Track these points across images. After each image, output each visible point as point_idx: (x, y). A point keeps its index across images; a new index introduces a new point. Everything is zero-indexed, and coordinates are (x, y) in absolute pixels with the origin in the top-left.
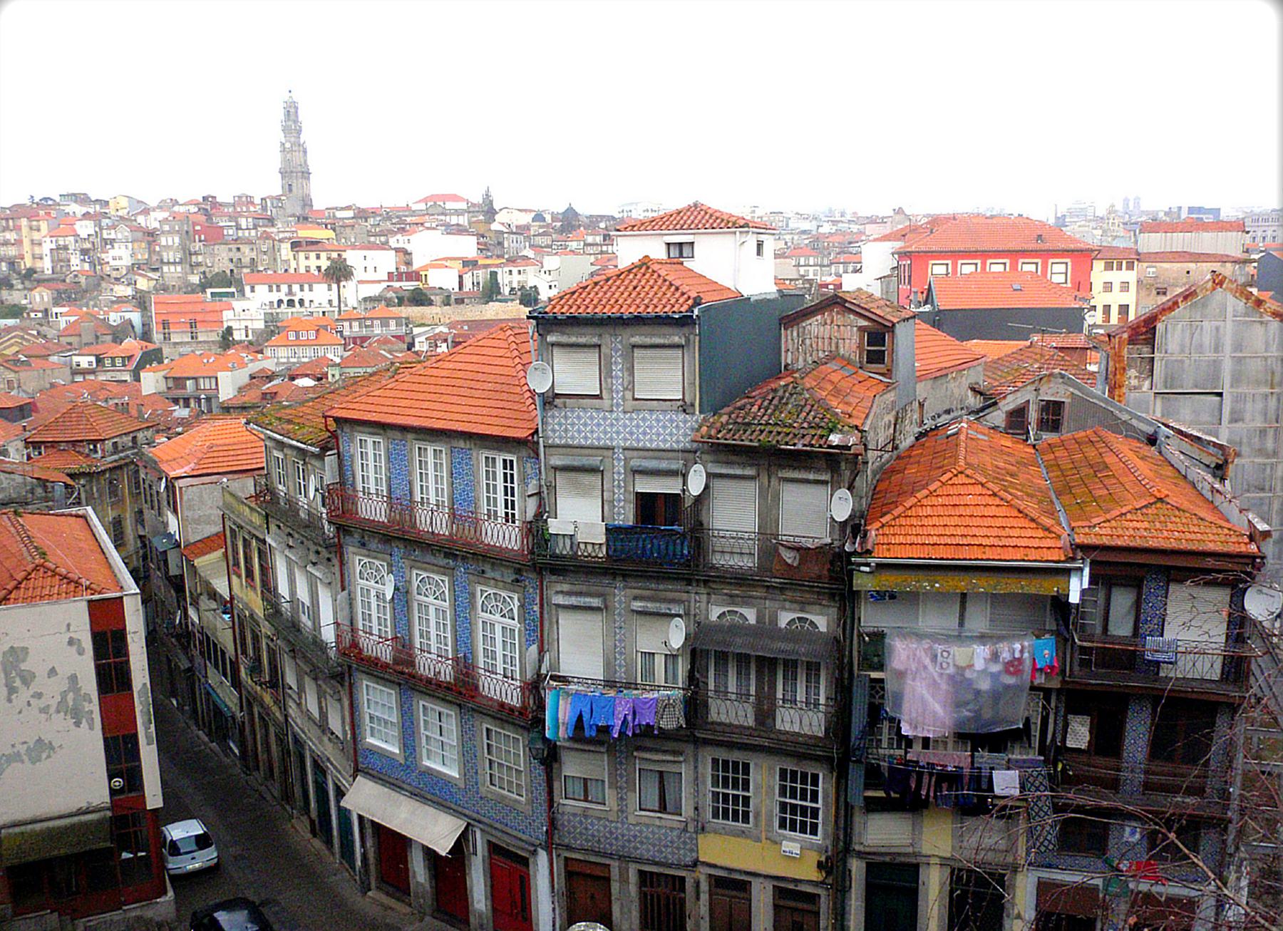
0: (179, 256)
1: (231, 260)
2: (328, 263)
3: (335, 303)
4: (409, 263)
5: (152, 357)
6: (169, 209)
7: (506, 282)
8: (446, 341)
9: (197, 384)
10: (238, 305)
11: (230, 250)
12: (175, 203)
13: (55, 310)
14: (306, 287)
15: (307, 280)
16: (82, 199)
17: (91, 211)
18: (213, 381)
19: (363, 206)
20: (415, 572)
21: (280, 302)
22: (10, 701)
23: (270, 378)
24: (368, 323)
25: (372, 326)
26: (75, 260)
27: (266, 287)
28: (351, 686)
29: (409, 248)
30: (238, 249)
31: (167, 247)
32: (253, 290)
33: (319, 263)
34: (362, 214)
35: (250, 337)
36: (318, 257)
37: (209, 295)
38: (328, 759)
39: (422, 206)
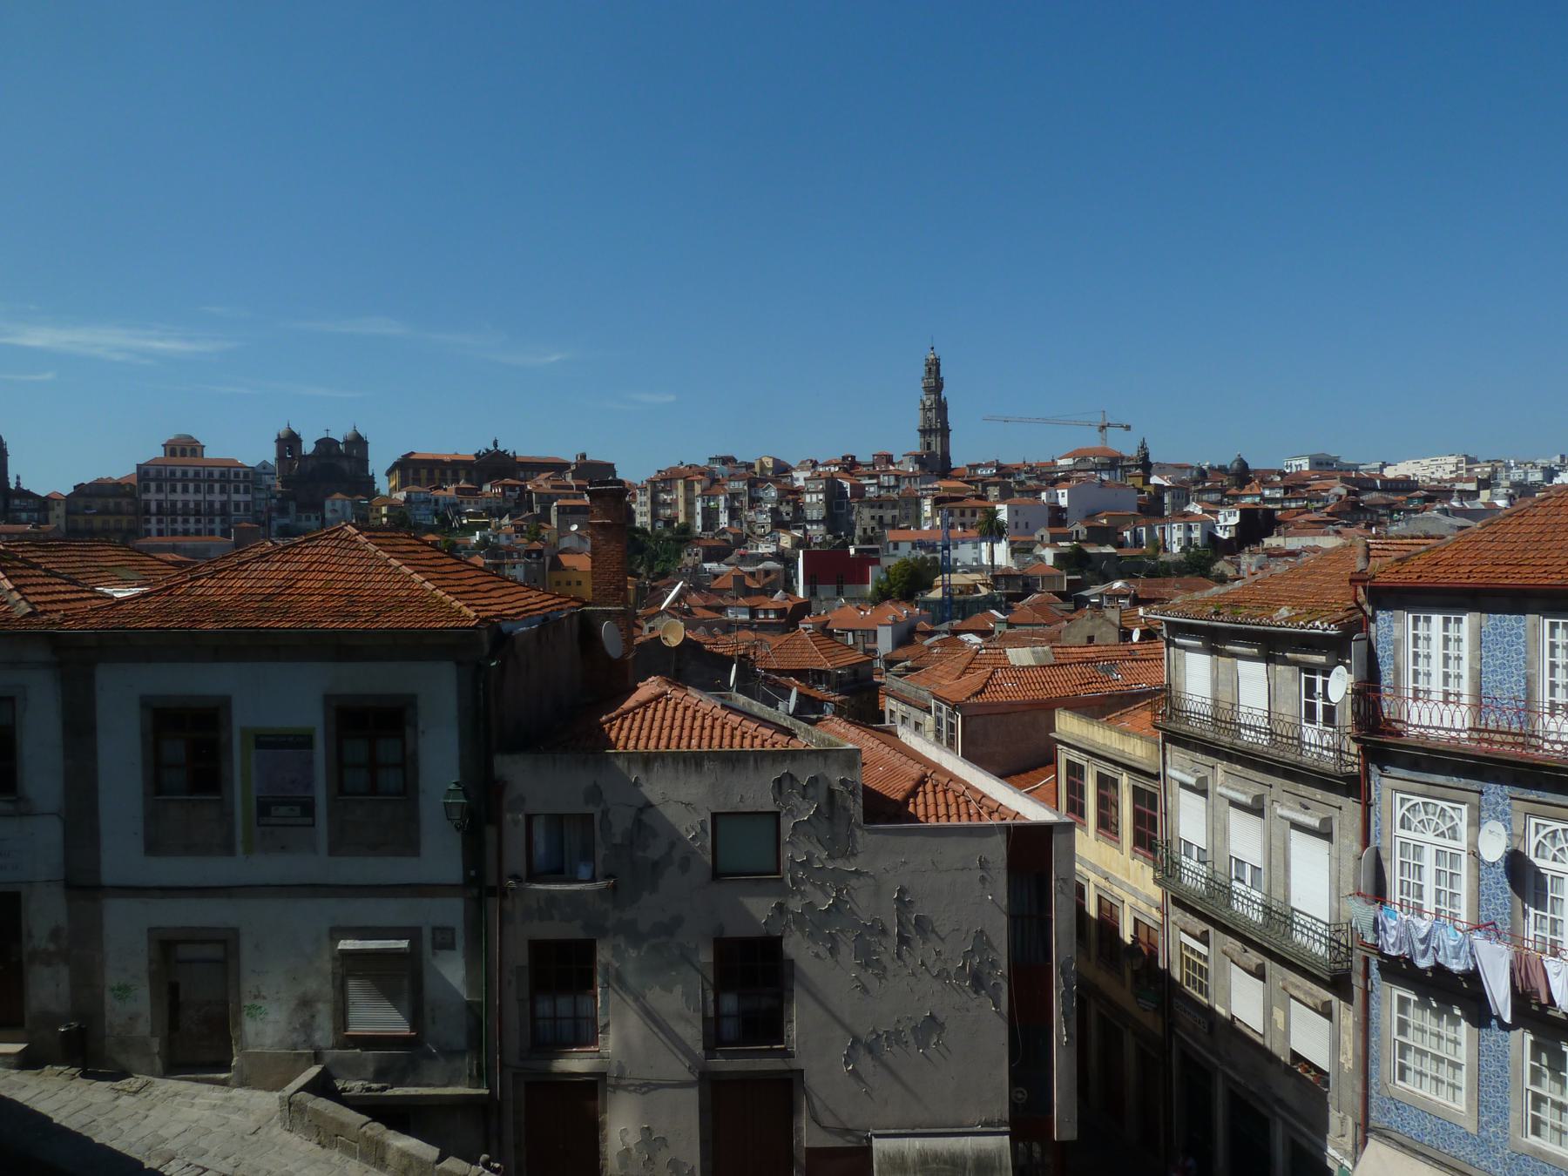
0: (823, 512)
1: (873, 518)
3: (985, 560)
5: (803, 609)
7: (1175, 539)
8: (1125, 596)
12: (815, 464)
13: (707, 566)
16: (726, 460)
19: (1004, 461)
20: (1533, 821)
22: (899, 956)
23: (930, 634)
26: (724, 519)
27: (909, 545)
28: (1367, 994)
29: (1063, 502)
31: (811, 504)
32: (896, 547)
33: (964, 520)
34: (1003, 471)
36: (963, 514)
37: (852, 551)
38: (1280, 1102)
39: (1070, 461)
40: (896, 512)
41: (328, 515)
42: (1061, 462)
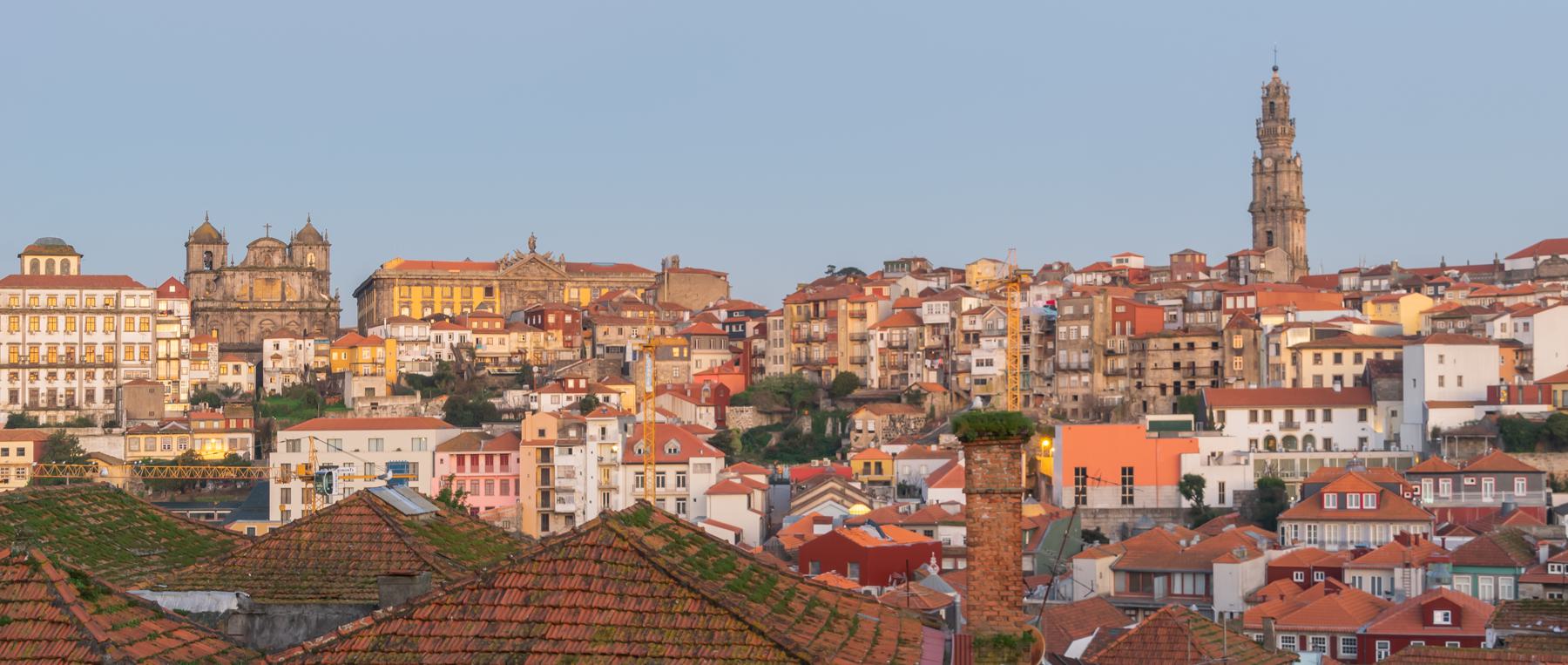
1: (1177, 366)
2: (1360, 369)
4: (1525, 371)
6: (1060, 281)
9: (1169, 585)
10: (1207, 443)
11: (1177, 347)
14: (1319, 413)
15: (1322, 399)
17: (933, 285)
18: (1201, 582)
21: (1270, 439)
24: (1467, 481)
25: (1478, 488)
29: (1525, 340)
30: (1191, 346)
31: (1068, 344)
33: (1338, 369)
35: (1229, 503)
39: (1527, 263)
40: (1216, 355)
41: (268, 364)
42: (1509, 266)
